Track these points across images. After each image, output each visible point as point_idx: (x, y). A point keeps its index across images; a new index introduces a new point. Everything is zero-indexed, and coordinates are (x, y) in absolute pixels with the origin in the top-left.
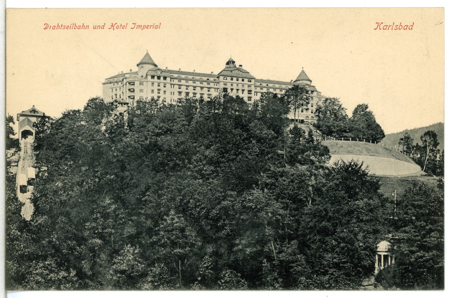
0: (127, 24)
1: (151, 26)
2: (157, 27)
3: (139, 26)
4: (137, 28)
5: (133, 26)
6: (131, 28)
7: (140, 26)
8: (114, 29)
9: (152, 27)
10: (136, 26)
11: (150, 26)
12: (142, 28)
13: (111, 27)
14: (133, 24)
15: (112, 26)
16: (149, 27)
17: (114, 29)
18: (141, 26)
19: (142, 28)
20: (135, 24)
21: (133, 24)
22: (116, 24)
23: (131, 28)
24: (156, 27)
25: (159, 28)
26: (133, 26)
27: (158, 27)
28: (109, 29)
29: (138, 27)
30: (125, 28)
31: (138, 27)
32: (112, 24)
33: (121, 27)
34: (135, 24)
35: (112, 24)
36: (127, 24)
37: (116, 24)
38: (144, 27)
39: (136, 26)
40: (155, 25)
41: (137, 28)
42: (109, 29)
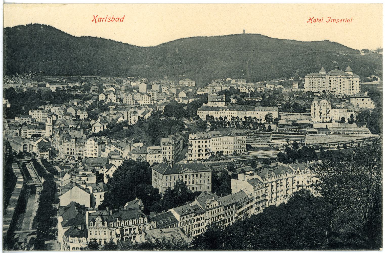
0: (323, 18)
1: (344, 20)
2: (348, 21)
3: (334, 20)
4: (331, 22)
5: (328, 20)
6: (327, 22)
7: (334, 20)
8: (311, 23)
9: (345, 21)
10: (331, 20)
11: (343, 21)
12: (336, 22)
13: (309, 21)
14: (328, 18)
15: (310, 20)
16: (342, 21)
17: (311, 23)
18: (335, 20)
19: (336, 22)
20: (330, 18)
21: (328, 18)
22: (313, 18)
23: (327, 22)
24: (348, 21)
27: (350, 21)
28: (308, 22)
29: (333, 20)
30: (321, 21)
31: (333, 20)
32: (310, 18)
33: (318, 21)
35: (310, 18)
36: (323, 18)
37: (313, 18)
38: (338, 21)
39: (331, 20)
40: (347, 20)
41: (331, 22)
42: (308, 22)
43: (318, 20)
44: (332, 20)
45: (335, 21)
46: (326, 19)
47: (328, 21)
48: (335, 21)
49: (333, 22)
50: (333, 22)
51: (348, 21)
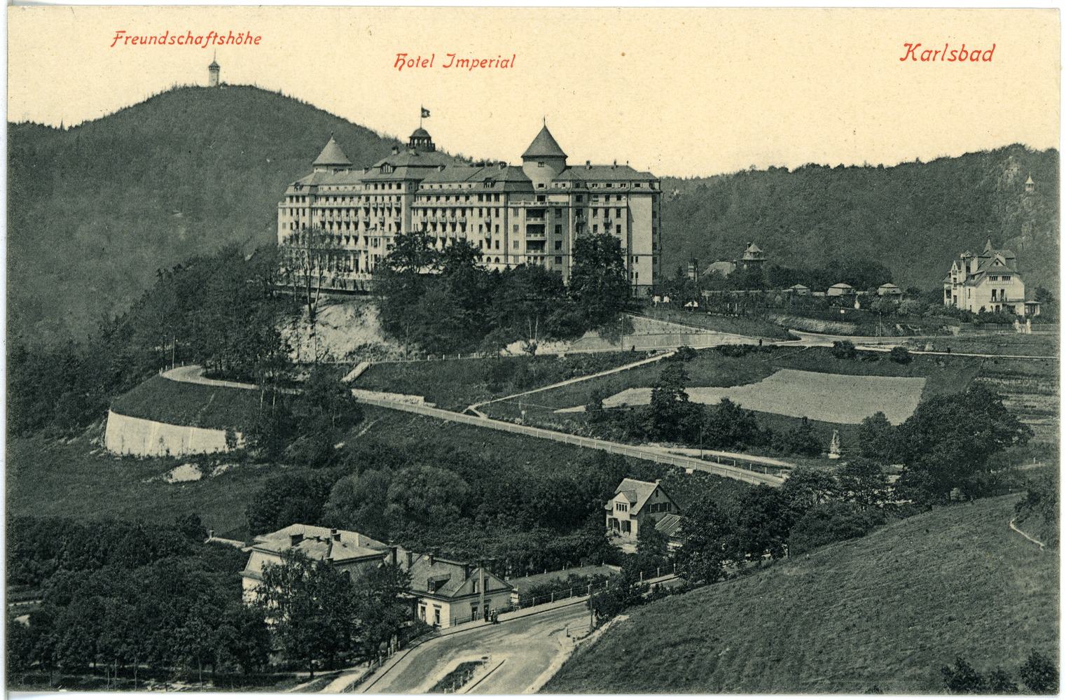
3: (463, 61)
4: (457, 66)
5: (448, 61)
6: (444, 66)
7: (464, 62)
10: (455, 62)
12: (470, 64)
14: (448, 55)
18: (468, 61)
19: (470, 64)
20: (454, 56)
21: (448, 55)
23: (444, 66)
25: (512, 66)
26: (448, 61)
29: (461, 63)
31: (461, 63)
34: (454, 56)
38: (476, 63)
39: (455, 62)
41: (457, 66)
43: (418, 60)
44: (458, 61)
45: (465, 63)
46: (442, 59)
47: (447, 64)
48: (465, 63)
49: (462, 66)
50: (462, 66)
51: (505, 64)
